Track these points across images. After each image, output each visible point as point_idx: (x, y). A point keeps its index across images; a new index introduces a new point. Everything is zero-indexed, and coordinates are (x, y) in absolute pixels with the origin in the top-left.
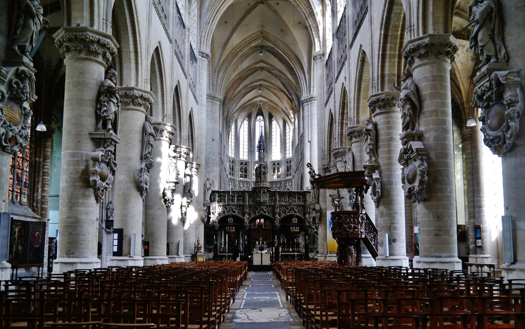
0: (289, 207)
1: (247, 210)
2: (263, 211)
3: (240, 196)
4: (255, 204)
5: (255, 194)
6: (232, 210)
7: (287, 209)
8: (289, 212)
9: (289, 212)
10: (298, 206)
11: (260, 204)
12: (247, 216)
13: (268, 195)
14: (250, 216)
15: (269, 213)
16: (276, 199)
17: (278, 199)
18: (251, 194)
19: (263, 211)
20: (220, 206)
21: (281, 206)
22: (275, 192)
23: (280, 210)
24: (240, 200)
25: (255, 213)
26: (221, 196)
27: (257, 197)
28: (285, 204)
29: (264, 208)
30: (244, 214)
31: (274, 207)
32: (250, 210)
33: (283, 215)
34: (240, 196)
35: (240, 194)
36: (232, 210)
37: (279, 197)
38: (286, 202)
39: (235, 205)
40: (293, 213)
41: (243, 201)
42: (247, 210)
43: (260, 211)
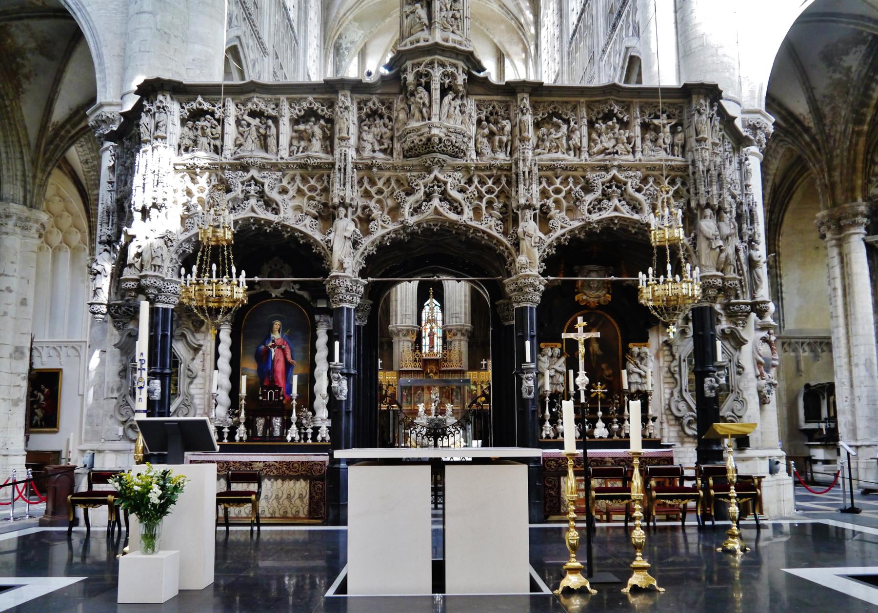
0: (599, 179)
1: (352, 194)
2: (445, 197)
3: (310, 115)
4: (397, 159)
5: (398, 103)
6: (261, 195)
7: (588, 188)
8: (597, 206)
9: (597, 206)
10: (650, 174)
11: (424, 150)
12: (346, 226)
13: (471, 104)
14: (367, 232)
15: (477, 210)
16: (518, 130)
17: (531, 133)
18: (374, 102)
19: (445, 197)
20: (192, 171)
21: (549, 171)
22: (512, 89)
23: (544, 194)
24: (309, 138)
25: (395, 211)
26: (197, 115)
27: (409, 115)
28: (571, 159)
29: (453, 181)
30: (327, 215)
31: (507, 178)
32: (367, 194)
33: (564, 224)
34: (310, 115)
35: (309, 101)
36: (261, 195)
37: (537, 125)
38: (578, 150)
39: (274, 166)
40: (626, 212)
41: (329, 148)
42: (352, 194)
43: (428, 197)
